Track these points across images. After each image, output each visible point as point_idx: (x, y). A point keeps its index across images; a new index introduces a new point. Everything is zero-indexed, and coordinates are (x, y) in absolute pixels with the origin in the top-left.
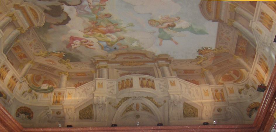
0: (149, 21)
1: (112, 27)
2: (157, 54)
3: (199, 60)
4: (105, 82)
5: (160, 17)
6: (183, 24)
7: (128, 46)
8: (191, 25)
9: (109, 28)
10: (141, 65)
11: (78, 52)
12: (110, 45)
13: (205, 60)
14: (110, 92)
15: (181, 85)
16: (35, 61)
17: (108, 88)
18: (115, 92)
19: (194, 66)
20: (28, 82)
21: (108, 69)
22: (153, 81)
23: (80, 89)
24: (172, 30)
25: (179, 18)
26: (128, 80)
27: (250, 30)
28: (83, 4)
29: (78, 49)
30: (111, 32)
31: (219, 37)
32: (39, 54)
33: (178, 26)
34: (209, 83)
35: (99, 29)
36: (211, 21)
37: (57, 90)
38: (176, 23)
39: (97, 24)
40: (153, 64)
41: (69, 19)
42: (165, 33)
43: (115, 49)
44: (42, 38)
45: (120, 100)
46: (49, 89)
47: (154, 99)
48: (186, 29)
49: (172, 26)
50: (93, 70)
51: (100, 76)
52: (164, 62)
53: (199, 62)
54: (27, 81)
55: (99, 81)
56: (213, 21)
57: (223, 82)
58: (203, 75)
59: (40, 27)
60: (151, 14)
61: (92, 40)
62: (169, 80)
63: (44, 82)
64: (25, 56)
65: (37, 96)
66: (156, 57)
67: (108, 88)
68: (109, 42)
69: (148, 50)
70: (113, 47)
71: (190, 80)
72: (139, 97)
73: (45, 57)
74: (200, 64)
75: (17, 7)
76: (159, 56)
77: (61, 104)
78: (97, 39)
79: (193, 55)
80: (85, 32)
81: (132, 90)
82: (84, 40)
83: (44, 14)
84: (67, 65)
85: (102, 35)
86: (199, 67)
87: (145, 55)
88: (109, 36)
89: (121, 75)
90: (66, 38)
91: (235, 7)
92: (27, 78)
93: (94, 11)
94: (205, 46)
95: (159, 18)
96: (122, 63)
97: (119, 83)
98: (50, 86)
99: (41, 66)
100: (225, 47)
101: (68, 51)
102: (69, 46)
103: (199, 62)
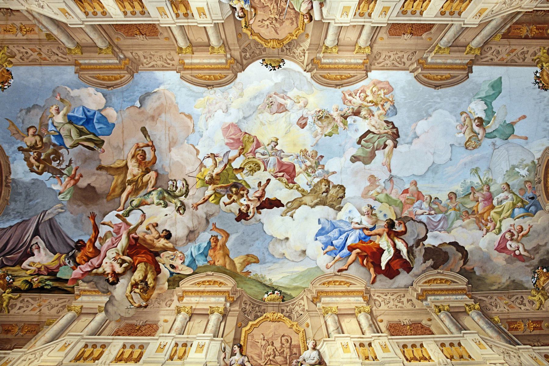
5: (461, 135)
27: (483, 25)
28: (425, 221)
60: (451, 145)
75: (422, 297)
95: (463, 137)
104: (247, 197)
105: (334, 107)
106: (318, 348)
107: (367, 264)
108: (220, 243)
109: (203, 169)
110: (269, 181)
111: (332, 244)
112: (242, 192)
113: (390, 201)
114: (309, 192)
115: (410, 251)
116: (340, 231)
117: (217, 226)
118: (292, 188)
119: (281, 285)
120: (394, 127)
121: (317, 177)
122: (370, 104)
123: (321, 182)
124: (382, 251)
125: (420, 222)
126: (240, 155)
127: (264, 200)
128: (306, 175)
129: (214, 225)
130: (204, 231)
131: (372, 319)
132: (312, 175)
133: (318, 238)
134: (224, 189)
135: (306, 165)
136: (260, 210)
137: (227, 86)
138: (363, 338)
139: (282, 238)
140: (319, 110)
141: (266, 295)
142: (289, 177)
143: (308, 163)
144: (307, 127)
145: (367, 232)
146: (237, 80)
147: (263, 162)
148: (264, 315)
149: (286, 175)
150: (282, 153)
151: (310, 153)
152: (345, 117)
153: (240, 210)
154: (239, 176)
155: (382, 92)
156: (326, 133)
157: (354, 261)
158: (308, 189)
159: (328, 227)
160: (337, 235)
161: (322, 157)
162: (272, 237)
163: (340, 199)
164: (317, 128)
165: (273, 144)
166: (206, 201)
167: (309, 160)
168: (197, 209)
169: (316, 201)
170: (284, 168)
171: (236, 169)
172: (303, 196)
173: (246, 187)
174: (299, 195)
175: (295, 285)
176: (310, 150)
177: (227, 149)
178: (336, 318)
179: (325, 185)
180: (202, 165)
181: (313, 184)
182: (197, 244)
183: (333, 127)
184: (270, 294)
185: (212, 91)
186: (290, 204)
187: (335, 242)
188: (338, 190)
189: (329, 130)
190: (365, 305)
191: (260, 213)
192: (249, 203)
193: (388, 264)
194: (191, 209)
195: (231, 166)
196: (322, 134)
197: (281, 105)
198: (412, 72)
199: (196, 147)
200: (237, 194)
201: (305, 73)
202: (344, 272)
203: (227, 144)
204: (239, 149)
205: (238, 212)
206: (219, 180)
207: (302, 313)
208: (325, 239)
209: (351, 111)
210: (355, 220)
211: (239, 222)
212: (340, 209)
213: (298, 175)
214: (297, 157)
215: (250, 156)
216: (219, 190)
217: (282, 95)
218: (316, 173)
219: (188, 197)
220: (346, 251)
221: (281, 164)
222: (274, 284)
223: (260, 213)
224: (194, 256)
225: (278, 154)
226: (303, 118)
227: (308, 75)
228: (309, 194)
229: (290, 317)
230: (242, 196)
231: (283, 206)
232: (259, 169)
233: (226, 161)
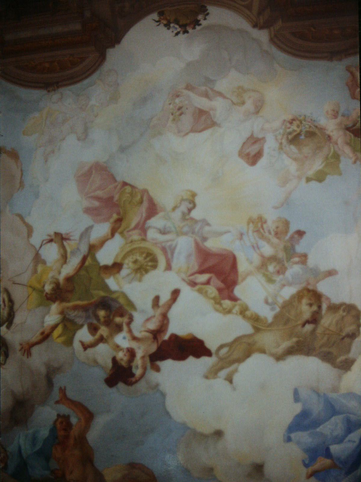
104: (130, 331)
105: (328, 107)
108: (75, 432)
109: (40, 268)
110: (176, 293)
111: (328, 454)
112: (118, 320)
114: (270, 320)
116: (348, 421)
117: (70, 394)
118: (229, 312)
121: (290, 284)
123: (299, 296)
126: (113, 235)
127: (166, 337)
128: (263, 280)
129: (63, 391)
130: (43, 402)
133: (293, 435)
134: (81, 313)
135: (262, 256)
136: (159, 363)
137: (86, 82)
139: (207, 430)
140: (290, 117)
142: (221, 285)
143: (268, 250)
144: (262, 162)
146: (107, 66)
147: (164, 250)
149: (217, 282)
150: (207, 228)
153: (114, 360)
154: (111, 282)
156: (311, 173)
160: (339, 431)
161: (300, 233)
163: (347, 340)
164: (288, 161)
165: (184, 207)
166: (46, 337)
167: (268, 241)
168: (29, 354)
169: (286, 344)
170: (211, 263)
171: (106, 268)
172: (257, 330)
173: (127, 308)
174: (245, 328)
177: (87, 221)
179: (311, 305)
180: (38, 259)
181: (280, 301)
182: (31, 431)
183: (327, 158)
185: (55, 96)
187: (335, 449)
188: (343, 317)
189: (317, 165)
191: (158, 369)
192: (134, 345)
194: (19, 354)
195: (94, 259)
196: (299, 178)
197: (201, 113)
199: (28, 220)
200: (108, 322)
201: (256, 33)
203: (88, 211)
204: (112, 220)
205: (110, 365)
206: (71, 291)
208: (310, 440)
211: (114, 390)
212: (347, 365)
213: (244, 279)
214: (242, 234)
215: (135, 236)
216: (72, 314)
217: (203, 88)
218: (289, 273)
219: (13, 327)
223: (158, 369)
224: (24, 455)
226: (253, 140)
227: (263, 36)
228: (271, 325)
230: (119, 328)
231: (208, 353)
232: (155, 267)
233: (84, 249)
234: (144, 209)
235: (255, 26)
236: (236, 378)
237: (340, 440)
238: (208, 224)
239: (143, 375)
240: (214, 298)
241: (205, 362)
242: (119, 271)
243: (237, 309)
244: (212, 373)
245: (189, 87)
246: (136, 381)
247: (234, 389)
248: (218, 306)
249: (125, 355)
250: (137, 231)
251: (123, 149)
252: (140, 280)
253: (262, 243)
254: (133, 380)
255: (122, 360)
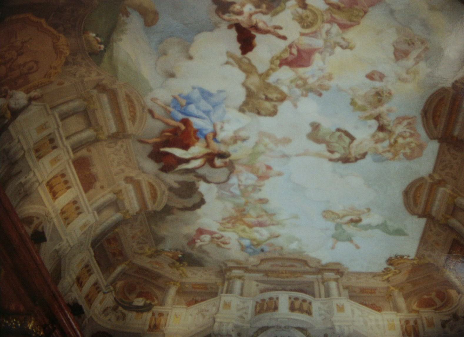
0: (324, 211)
1: (264, 219)
2: (324, 262)
3: (387, 274)
4: (234, 300)
6: (374, 219)
7: (282, 248)
8: (385, 221)
9: (260, 219)
10: (297, 277)
11: (204, 252)
12: (254, 245)
13: (395, 274)
14: (241, 317)
15: (352, 311)
16: (134, 261)
17: (238, 310)
18: (249, 317)
19: (378, 283)
20: (115, 293)
21: (244, 280)
22: (310, 303)
23: (194, 309)
24: (354, 226)
25: (369, 210)
26: (271, 299)
29: (205, 248)
30: (261, 225)
31: (424, 240)
32: (140, 252)
33: (365, 221)
34: (397, 309)
35: (246, 220)
36: (416, 216)
37: (157, 309)
38: (363, 217)
39: (244, 213)
40: (315, 276)
41: (202, 202)
42: (344, 231)
43: (262, 250)
44: (154, 227)
45: (255, 330)
46: (145, 305)
47: (309, 331)
48: (378, 227)
49: (356, 222)
50: (219, 281)
51: (229, 291)
52: (332, 275)
53: (386, 277)
54: (113, 292)
55: (225, 298)
56: (420, 216)
57: (417, 309)
58: (389, 296)
59: (155, 212)
61: (231, 236)
62: (335, 302)
63: (139, 295)
64: (121, 253)
65: (124, 316)
66: (322, 266)
67: (238, 310)
68: (255, 240)
69: (313, 255)
70: (259, 248)
71: (367, 303)
72: (285, 327)
73: (151, 256)
74: (388, 280)
75: (129, 180)
76: (327, 265)
77: (162, 331)
78: (238, 234)
79: (380, 266)
80: (221, 224)
81: (276, 315)
82: (217, 236)
83: (167, 192)
84: (180, 271)
85: (247, 229)
86: (385, 284)
87: (305, 263)
88: (257, 232)
89: (262, 291)
90: (190, 230)
91: (456, 198)
92: (115, 288)
93: (244, 192)
94: (400, 253)
95: (339, 209)
96: (266, 273)
97: (257, 303)
98: (148, 302)
99: (141, 270)
100: (430, 256)
101: (188, 250)
102: (192, 242)
103: (386, 277)
106: (33, 103)
107: (165, 136)
110: (284, 38)
111: (188, 104)
112: (264, 6)
113: (254, 154)
115: (188, 171)
119: (114, 51)
120: (356, 159)
122: (392, 141)
123: (281, 93)
124: (186, 147)
125: (228, 178)
127: (253, 32)
131: (88, 142)
132: (293, 85)
133: (197, 90)
135: (307, 79)
138: (61, 139)
141: (94, 35)
144: (368, 81)
145: (211, 136)
147: (315, 32)
148: (61, 35)
149: (291, 58)
151: (326, 83)
152: (377, 118)
155: (408, 151)
157: (167, 124)
158: (271, 80)
159: (215, 100)
162: (192, 41)
163: (256, 111)
165: (343, 43)
169: (253, 88)
170: (304, 55)
172: (260, 75)
175: (120, 69)
176: (333, 83)
178: (81, 110)
184: (97, 40)
186: (247, 61)
189: (360, 103)
190: (106, 133)
193: (167, 154)
198: (430, 176)
202: (149, 116)
204: (340, 4)
207: (78, 75)
209: (385, 122)
210: (226, 126)
215: (327, 17)
220: (181, 116)
221: (311, 52)
222: (114, 44)
223: (230, 27)
225: (330, 47)
226: (382, 77)
228: (264, 81)
229: (67, 63)
234: (345, 22)
235: (456, 81)
236: (228, 67)
237: (198, 108)
238: (330, 55)
239: (225, 20)
240: (280, 56)
241: (238, 53)
242: (300, 7)
243: (273, 66)
244: (230, 55)
245: (427, 49)
246: (220, 16)
247: (222, 65)
248: (275, 58)
249: (238, 9)
250: (330, 18)
251: (392, 12)
252: (293, 19)
253: (316, 79)
254: (220, 14)
255: (234, 7)
